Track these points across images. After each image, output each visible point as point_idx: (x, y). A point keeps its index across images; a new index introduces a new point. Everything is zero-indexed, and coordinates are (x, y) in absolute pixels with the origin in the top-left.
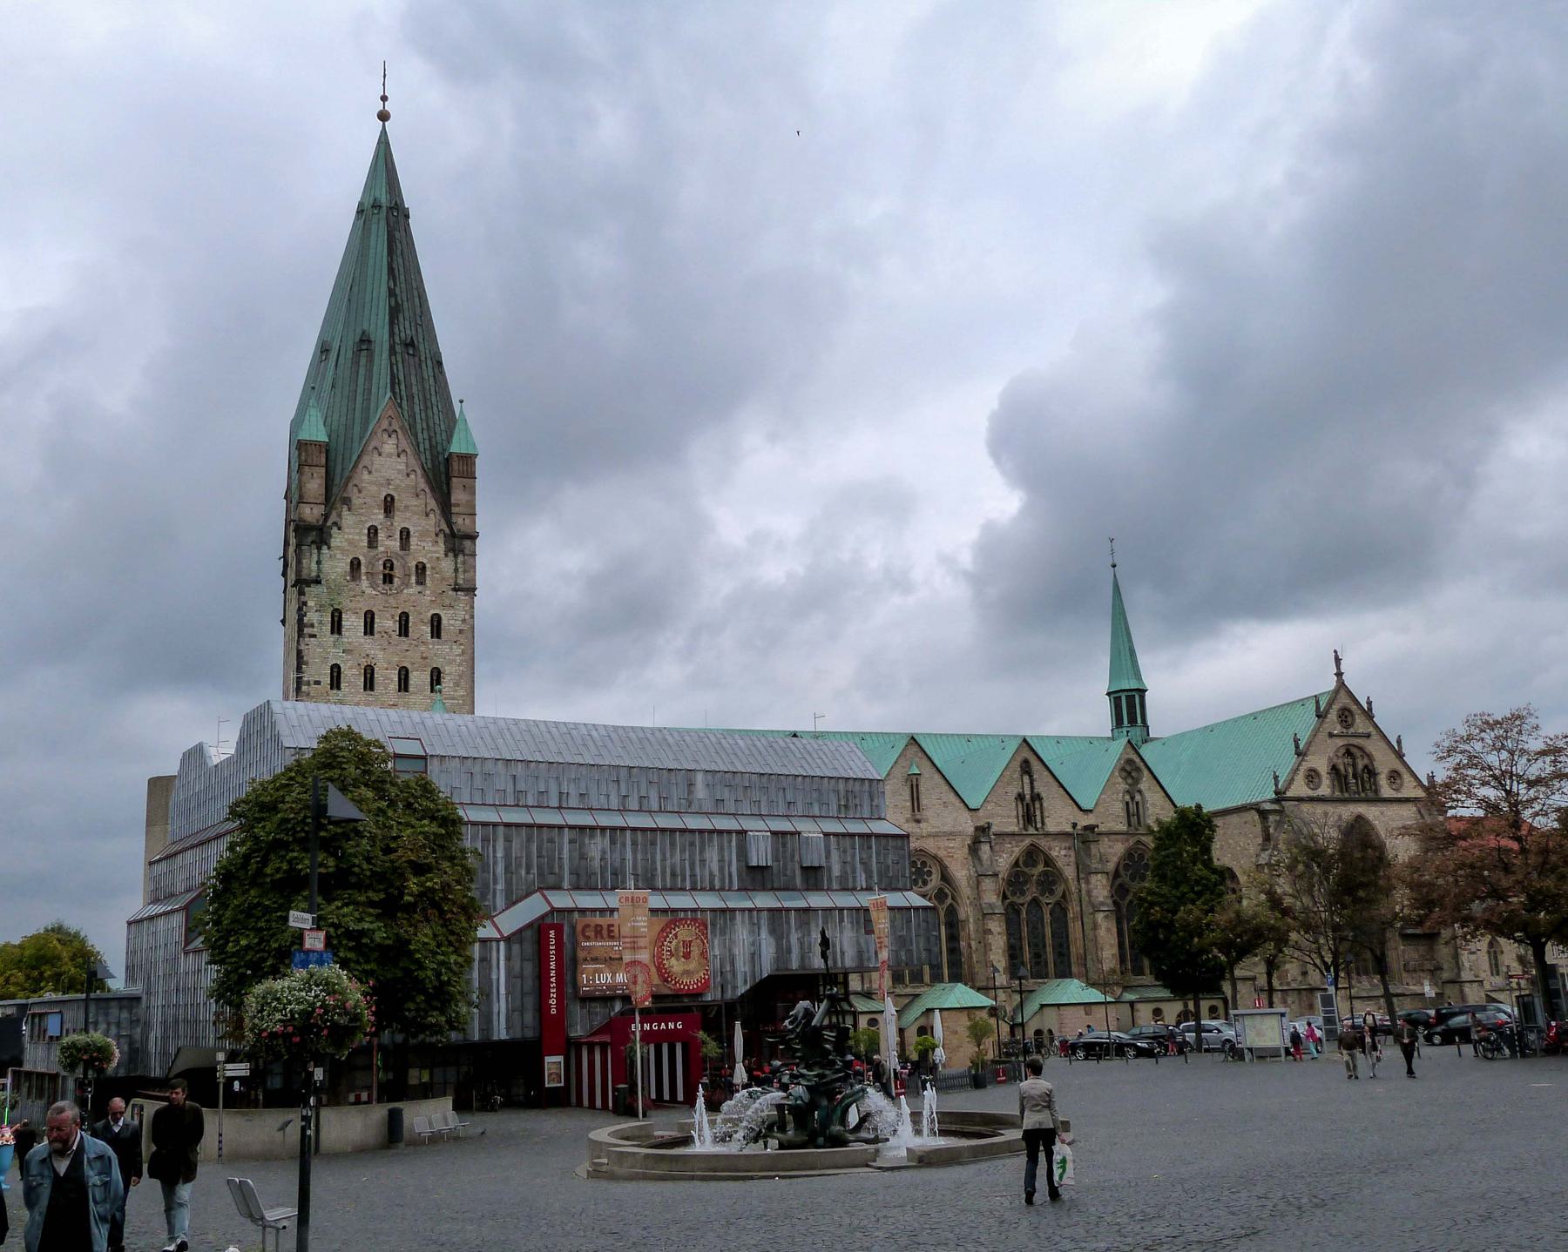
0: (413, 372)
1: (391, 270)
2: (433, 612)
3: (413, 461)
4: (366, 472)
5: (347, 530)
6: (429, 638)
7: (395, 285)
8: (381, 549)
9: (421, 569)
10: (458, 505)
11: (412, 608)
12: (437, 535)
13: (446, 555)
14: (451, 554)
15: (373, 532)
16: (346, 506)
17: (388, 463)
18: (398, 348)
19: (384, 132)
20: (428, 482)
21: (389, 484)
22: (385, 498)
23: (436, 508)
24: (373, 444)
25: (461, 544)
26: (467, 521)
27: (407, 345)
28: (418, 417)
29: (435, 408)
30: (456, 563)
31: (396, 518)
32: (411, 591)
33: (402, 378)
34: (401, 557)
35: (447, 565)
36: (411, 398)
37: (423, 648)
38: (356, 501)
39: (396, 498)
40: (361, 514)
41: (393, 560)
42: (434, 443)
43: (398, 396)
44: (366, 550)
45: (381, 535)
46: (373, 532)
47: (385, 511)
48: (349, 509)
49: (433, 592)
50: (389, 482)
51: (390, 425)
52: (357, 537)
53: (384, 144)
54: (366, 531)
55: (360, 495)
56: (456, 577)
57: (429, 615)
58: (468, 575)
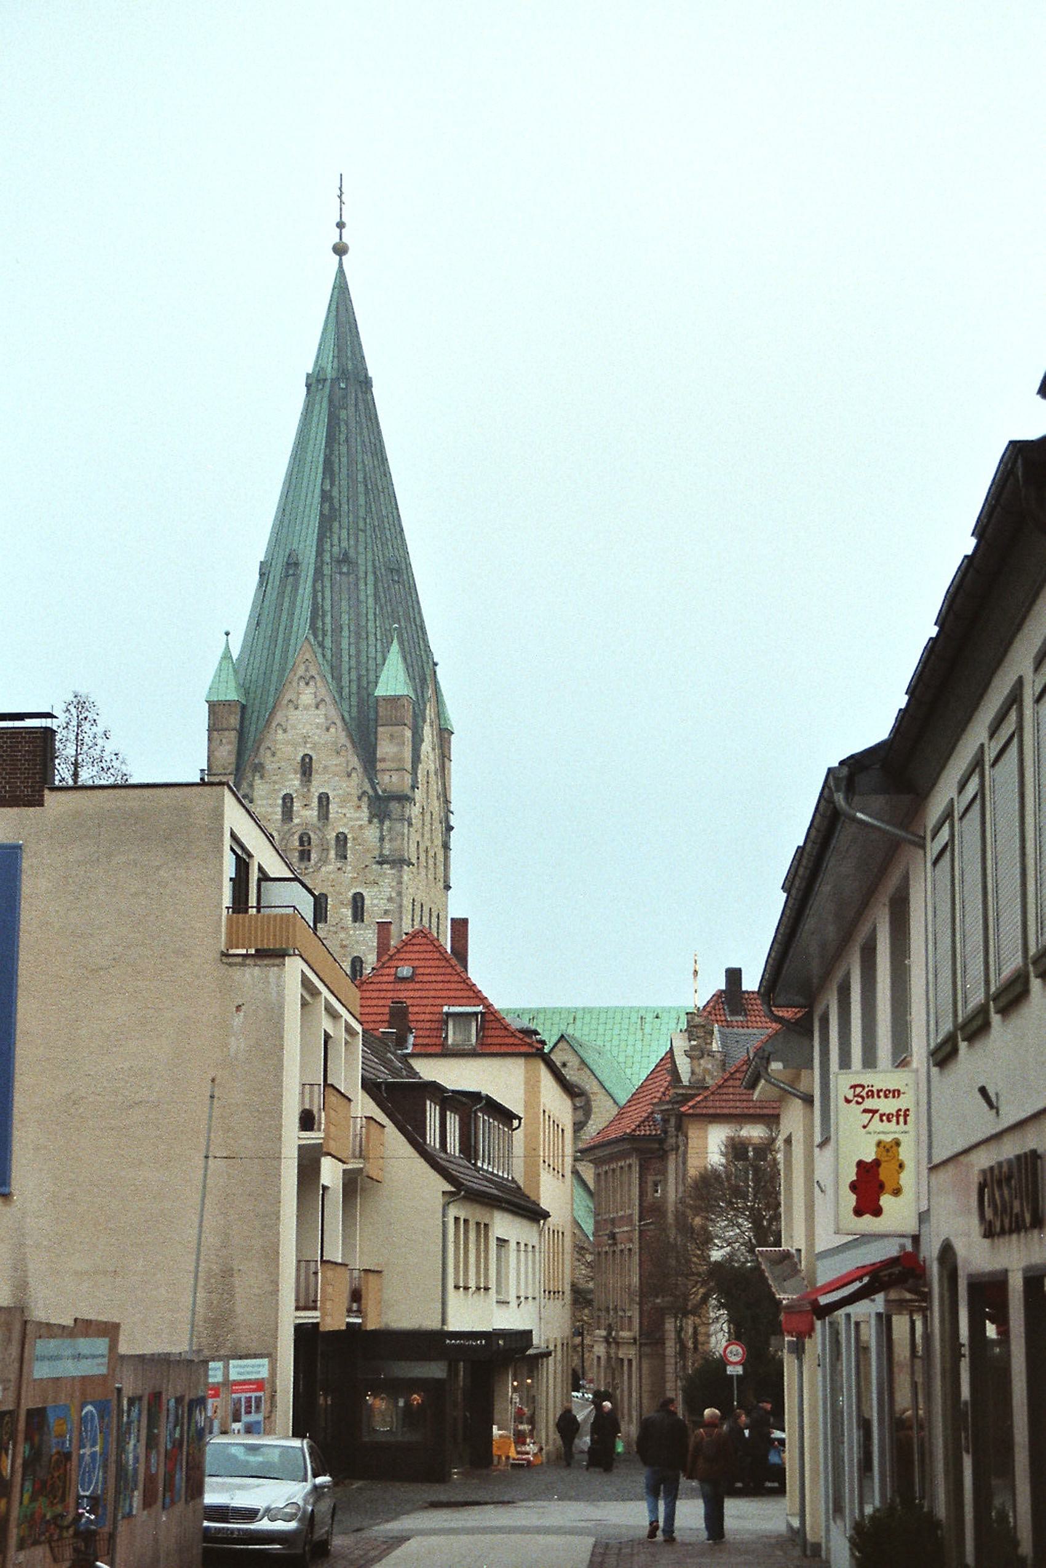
0: (345, 596)
1: (328, 463)
2: (353, 891)
3: (333, 712)
4: (280, 732)
5: (259, 802)
6: (350, 922)
7: (332, 484)
8: (296, 821)
9: (341, 840)
10: (383, 760)
11: (330, 889)
12: (360, 798)
13: (370, 822)
14: (375, 820)
15: (288, 800)
16: (258, 774)
17: (305, 717)
18: (327, 570)
19: (341, 271)
20: (350, 736)
21: (305, 743)
22: (303, 759)
23: (357, 766)
24: (287, 697)
25: (387, 806)
26: (394, 778)
27: (339, 562)
28: (345, 654)
29: (372, 638)
30: (382, 830)
31: (314, 783)
32: (331, 868)
33: (328, 607)
34: (319, 829)
35: (371, 833)
36: (338, 629)
37: (342, 935)
38: (270, 765)
39: (314, 758)
40: (275, 782)
41: (310, 833)
42: (364, 684)
43: (320, 633)
44: (279, 823)
45: (297, 806)
46: (288, 800)
47: (304, 773)
48: (262, 777)
49: (354, 867)
50: (305, 739)
51: (307, 670)
52: (270, 810)
53: (341, 291)
54: (280, 802)
55: (274, 759)
56: (381, 848)
57: (350, 894)
58: (397, 844)
